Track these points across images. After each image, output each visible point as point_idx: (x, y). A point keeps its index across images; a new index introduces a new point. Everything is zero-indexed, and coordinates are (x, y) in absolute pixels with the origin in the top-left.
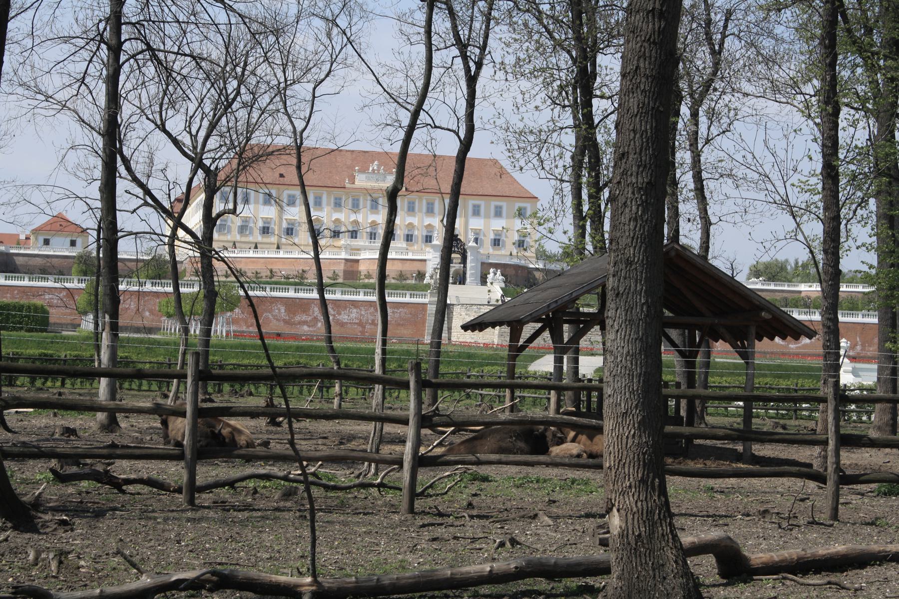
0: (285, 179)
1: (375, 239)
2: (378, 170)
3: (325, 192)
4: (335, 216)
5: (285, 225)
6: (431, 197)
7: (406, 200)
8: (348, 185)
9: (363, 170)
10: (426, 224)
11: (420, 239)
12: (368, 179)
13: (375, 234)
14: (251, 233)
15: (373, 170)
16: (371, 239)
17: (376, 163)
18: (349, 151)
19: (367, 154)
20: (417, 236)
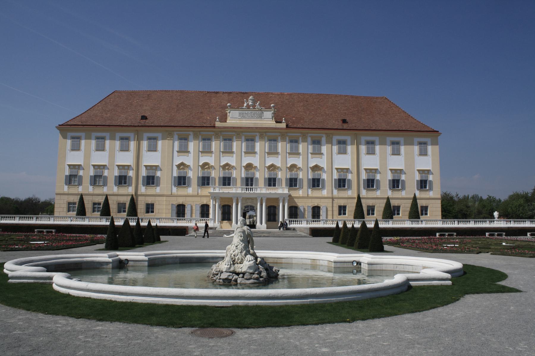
0: (147, 121)
1: (252, 185)
2: (254, 106)
3: (191, 133)
4: (204, 159)
5: (143, 172)
6: (316, 134)
7: (287, 138)
8: (218, 124)
9: (237, 106)
10: (312, 164)
11: (305, 183)
12: (243, 117)
13: (252, 179)
14: (105, 184)
15: (248, 107)
16: (247, 185)
17: (251, 97)
18: (226, 93)
19: (246, 95)
20: (301, 180)
